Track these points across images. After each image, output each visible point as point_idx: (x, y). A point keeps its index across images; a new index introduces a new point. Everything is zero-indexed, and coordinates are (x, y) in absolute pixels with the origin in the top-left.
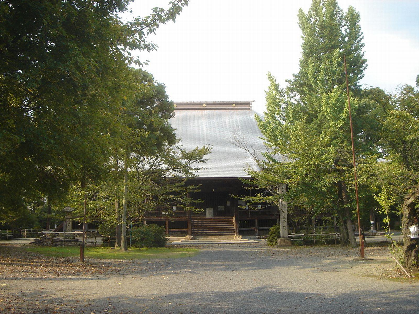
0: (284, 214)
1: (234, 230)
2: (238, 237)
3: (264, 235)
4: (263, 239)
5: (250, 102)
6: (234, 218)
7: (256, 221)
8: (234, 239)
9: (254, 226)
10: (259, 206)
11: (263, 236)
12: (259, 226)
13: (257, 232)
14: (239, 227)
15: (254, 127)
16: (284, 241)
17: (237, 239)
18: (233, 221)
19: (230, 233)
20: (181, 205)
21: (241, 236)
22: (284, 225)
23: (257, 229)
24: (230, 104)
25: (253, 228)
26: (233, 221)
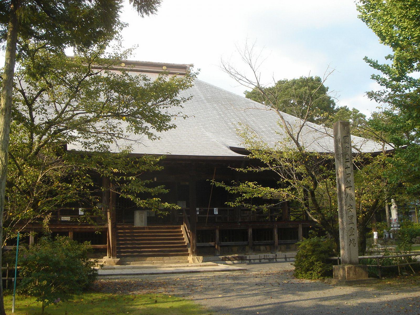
0: (350, 214)
1: (186, 246)
2: (196, 260)
3: (230, 255)
4: (230, 260)
5: (188, 66)
6: (183, 228)
7: (217, 232)
8: (188, 262)
9: (213, 240)
10: (215, 209)
11: (230, 256)
12: (222, 239)
13: (218, 250)
14: (198, 241)
15: (198, 96)
16: (355, 271)
17: (193, 262)
18: (181, 232)
19: (181, 251)
20: (129, 196)
21: (201, 258)
22: (352, 237)
23: (218, 245)
24: (160, 66)
25: (212, 244)
26: (181, 232)
